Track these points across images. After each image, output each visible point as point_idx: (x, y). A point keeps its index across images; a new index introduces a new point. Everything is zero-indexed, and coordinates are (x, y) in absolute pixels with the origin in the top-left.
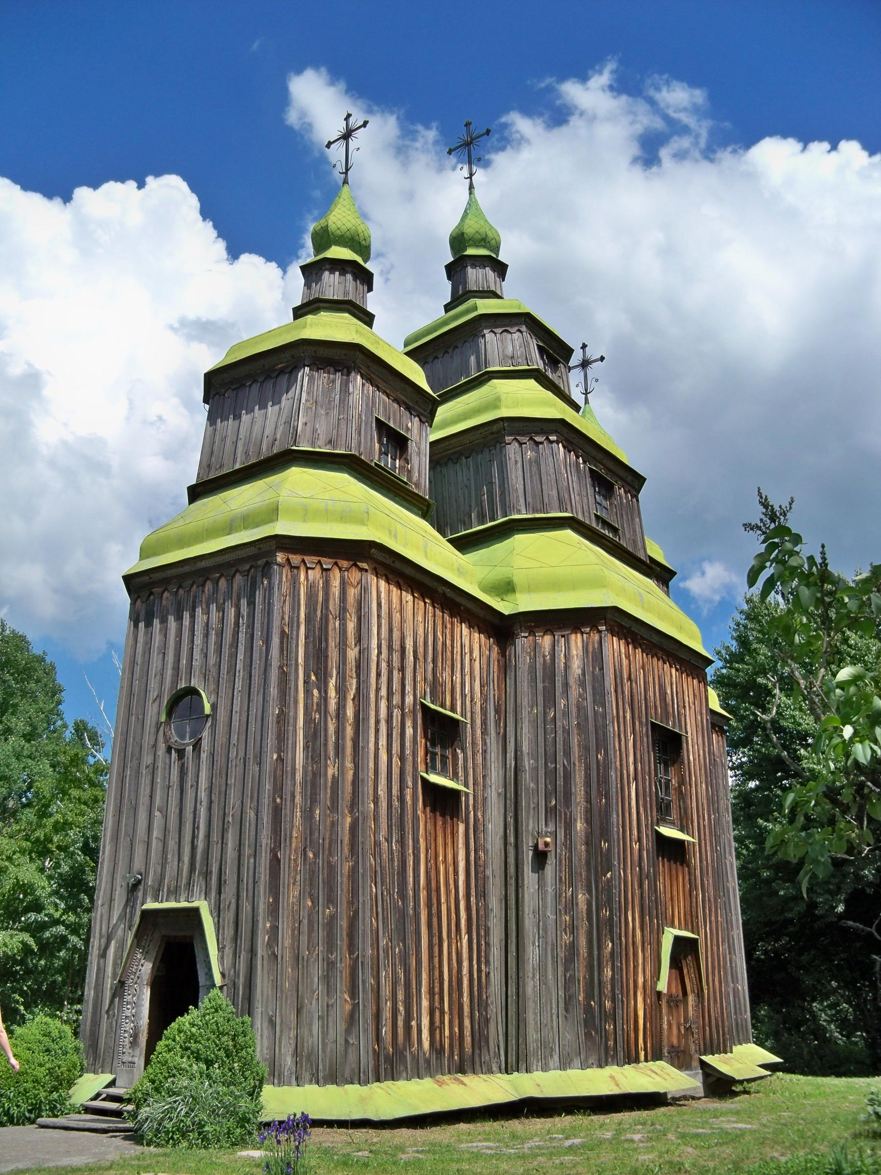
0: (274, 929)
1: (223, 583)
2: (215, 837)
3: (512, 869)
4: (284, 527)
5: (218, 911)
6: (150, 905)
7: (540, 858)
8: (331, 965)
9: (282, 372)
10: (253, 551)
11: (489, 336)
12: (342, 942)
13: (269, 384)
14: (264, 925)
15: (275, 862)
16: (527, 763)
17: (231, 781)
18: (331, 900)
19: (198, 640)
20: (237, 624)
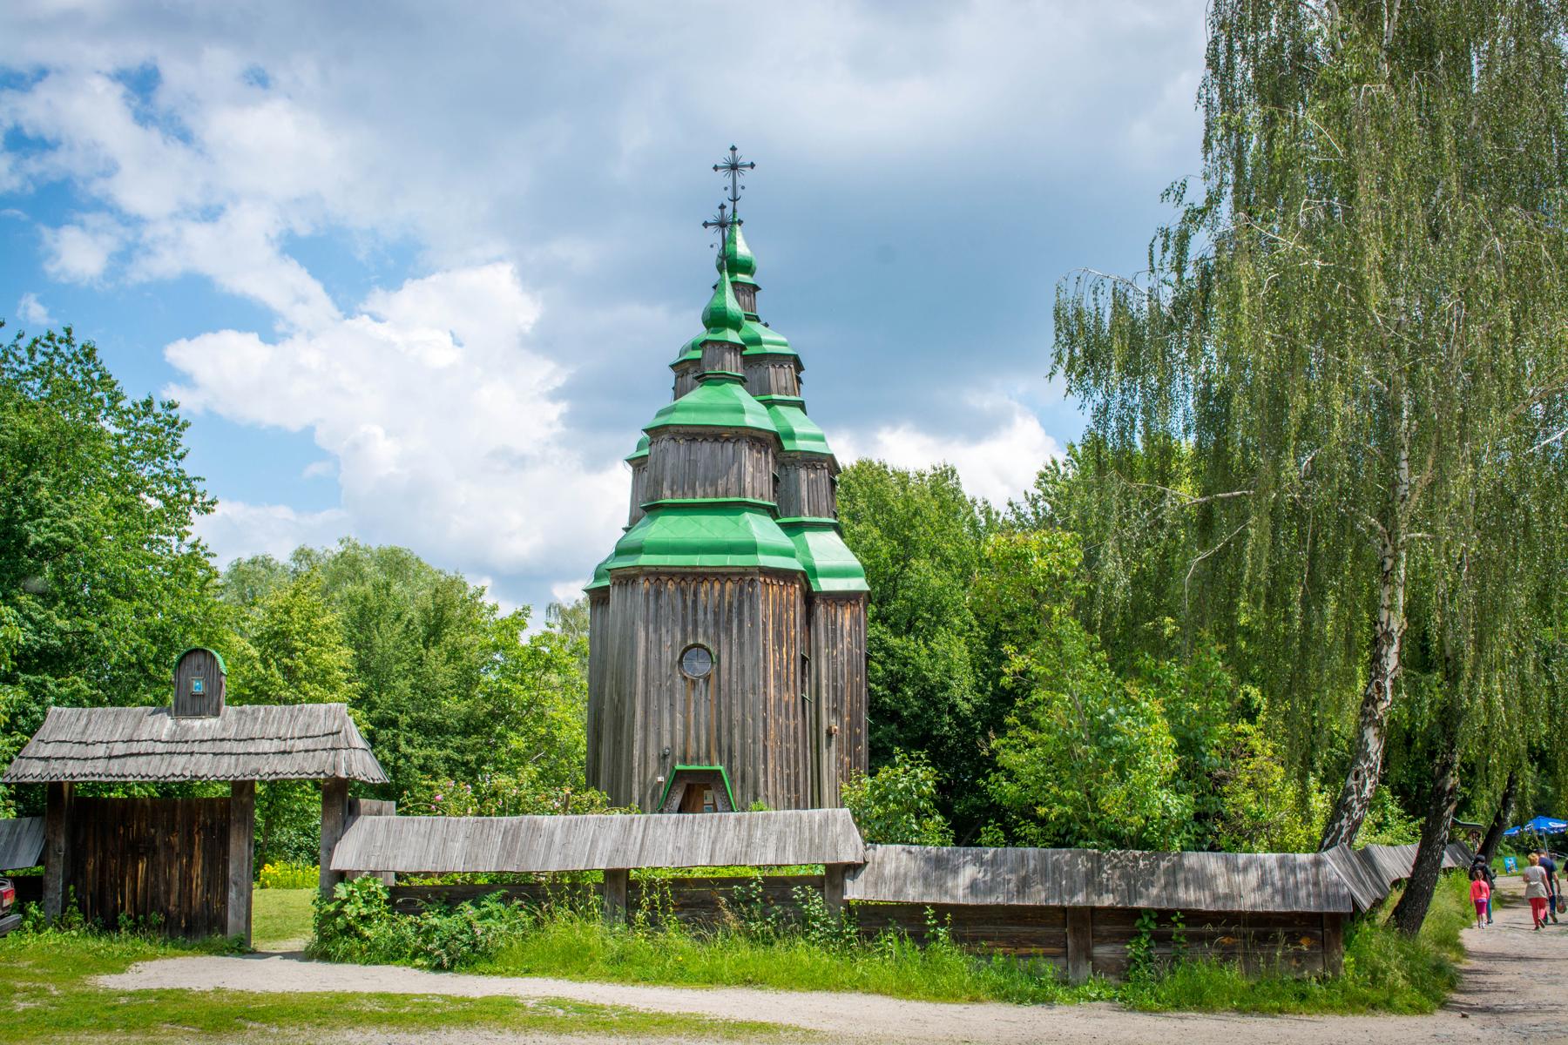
0: (766, 782)
1: (717, 586)
2: (724, 732)
3: (814, 743)
4: (764, 560)
5: (730, 769)
6: (679, 767)
7: (829, 734)
8: (789, 799)
9: (728, 440)
10: (742, 570)
11: (772, 370)
12: (793, 789)
13: (718, 445)
14: (762, 780)
15: (765, 747)
16: (824, 682)
17: (734, 702)
18: (788, 767)
19: (701, 616)
20: (730, 611)
